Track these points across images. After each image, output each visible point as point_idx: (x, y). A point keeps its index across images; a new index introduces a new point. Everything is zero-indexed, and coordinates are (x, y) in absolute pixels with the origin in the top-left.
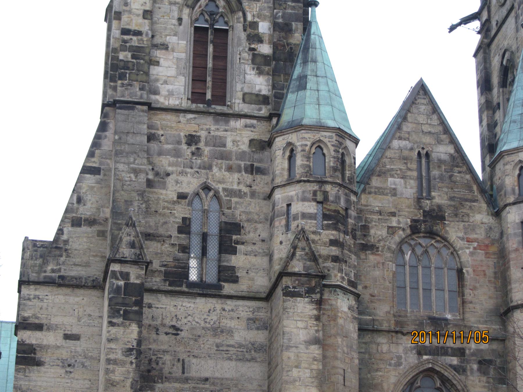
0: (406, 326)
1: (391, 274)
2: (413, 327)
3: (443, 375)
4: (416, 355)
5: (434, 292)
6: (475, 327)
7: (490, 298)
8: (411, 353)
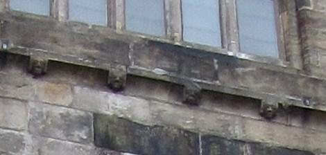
4: (91, 147)
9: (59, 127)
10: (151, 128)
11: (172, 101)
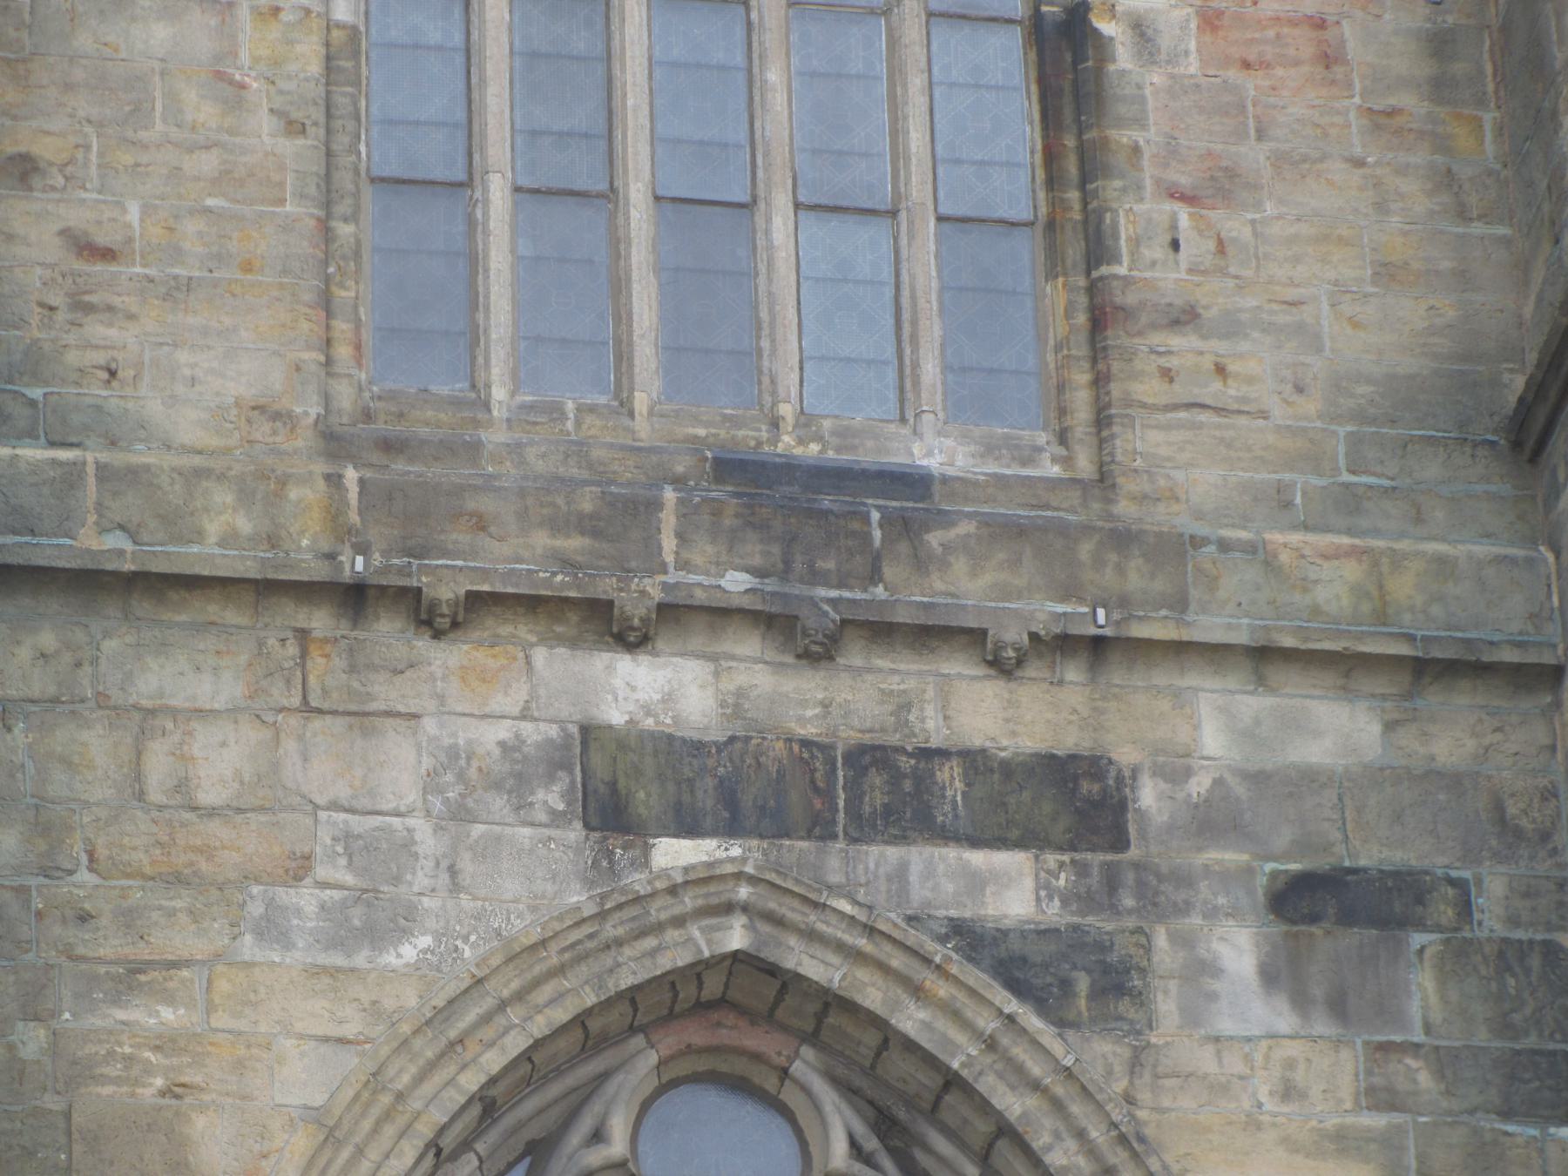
0: (459, 536)
1: (308, 57)
2: (542, 540)
3: (888, 1037)
4: (575, 833)
5: (780, 223)
6: (1224, 546)
7: (1387, 273)
8: (521, 807)
9: (497, 786)
10: (720, 746)
11: (770, 655)
